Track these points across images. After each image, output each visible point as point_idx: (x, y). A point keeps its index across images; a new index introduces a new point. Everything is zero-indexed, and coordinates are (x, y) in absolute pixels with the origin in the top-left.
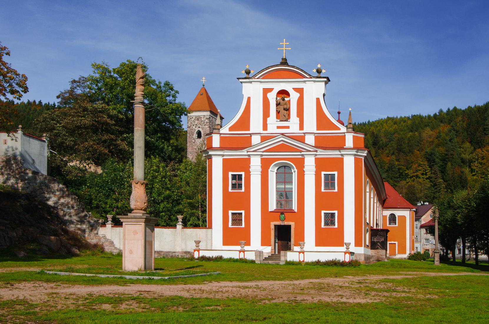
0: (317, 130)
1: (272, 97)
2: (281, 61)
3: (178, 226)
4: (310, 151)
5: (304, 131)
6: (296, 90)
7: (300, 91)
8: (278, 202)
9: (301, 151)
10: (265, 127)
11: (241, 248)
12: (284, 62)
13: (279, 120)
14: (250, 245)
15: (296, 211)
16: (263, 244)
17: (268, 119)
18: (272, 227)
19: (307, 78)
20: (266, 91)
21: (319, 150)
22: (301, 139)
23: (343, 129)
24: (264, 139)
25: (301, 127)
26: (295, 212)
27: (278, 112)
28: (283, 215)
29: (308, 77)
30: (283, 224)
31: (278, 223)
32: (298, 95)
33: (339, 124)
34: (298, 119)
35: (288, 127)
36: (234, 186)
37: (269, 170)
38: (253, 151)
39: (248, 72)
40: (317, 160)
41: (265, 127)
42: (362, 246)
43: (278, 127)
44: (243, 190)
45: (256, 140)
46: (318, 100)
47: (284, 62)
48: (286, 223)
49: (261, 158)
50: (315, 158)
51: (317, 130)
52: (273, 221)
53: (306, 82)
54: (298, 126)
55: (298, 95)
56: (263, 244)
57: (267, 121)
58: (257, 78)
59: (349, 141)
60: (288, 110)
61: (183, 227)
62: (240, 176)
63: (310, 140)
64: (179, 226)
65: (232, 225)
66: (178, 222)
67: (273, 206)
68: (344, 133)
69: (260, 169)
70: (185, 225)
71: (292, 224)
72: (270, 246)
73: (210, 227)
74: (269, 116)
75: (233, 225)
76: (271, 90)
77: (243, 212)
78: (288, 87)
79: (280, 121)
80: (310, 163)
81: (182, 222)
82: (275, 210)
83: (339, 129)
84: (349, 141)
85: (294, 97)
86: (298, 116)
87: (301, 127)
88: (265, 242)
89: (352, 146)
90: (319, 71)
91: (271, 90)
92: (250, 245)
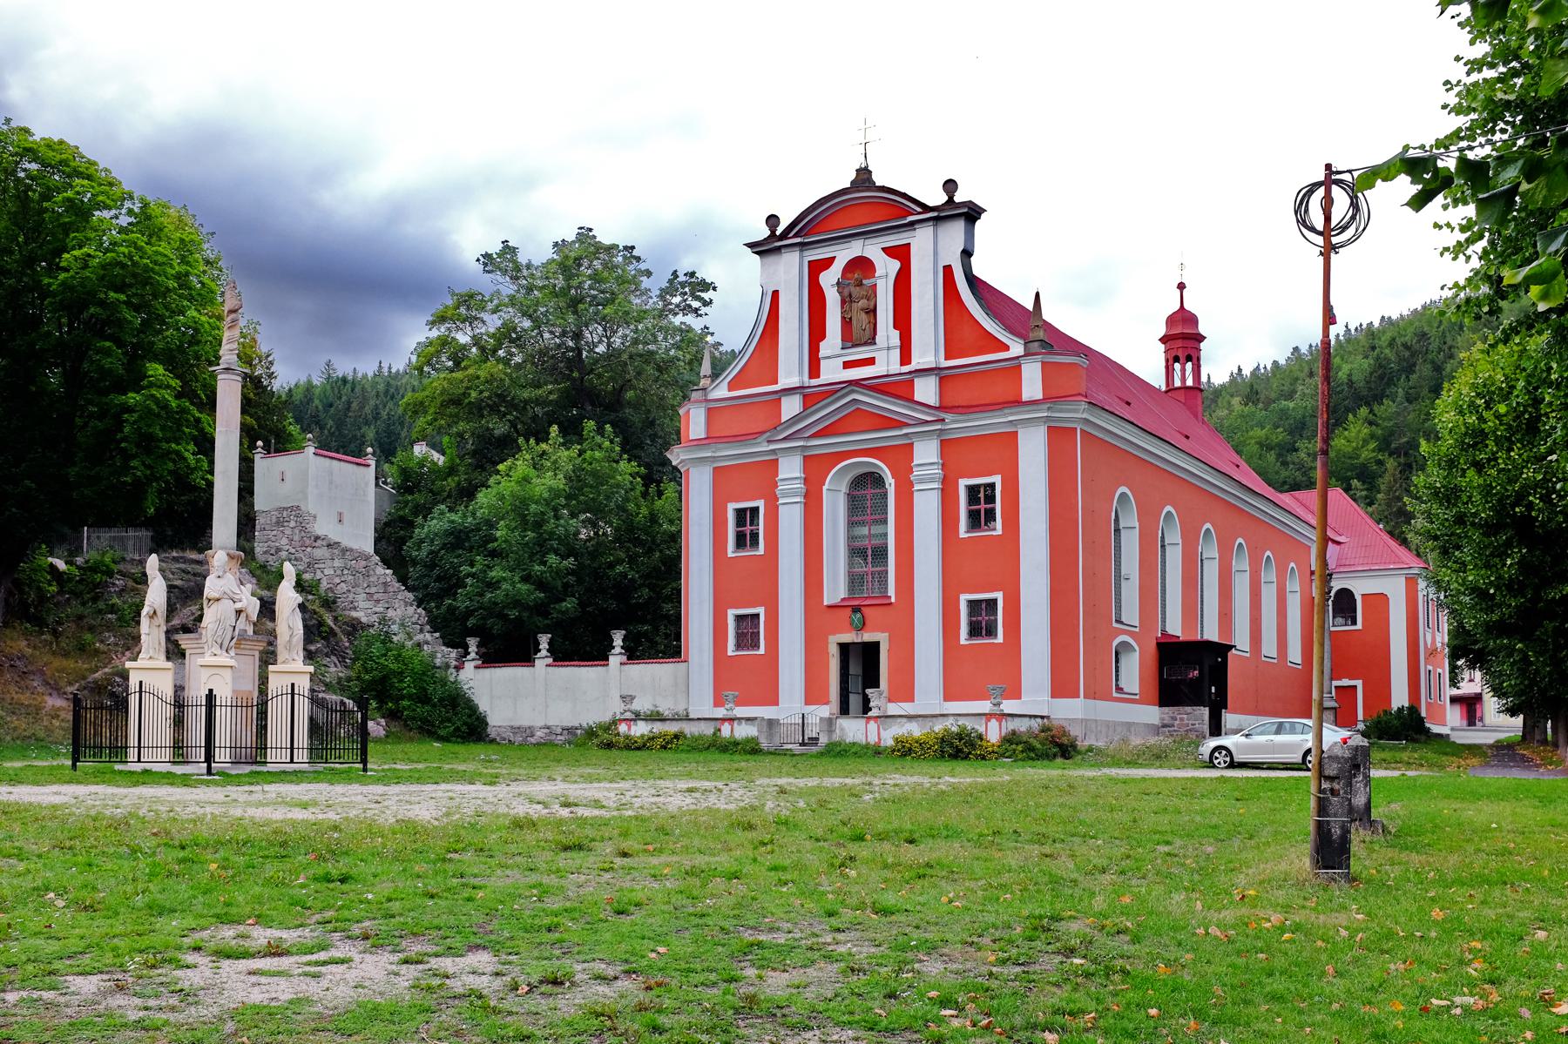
0: (947, 358)
1: (829, 280)
2: (853, 175)
3: (611, 658)
4: (927, 422)
5: (913, 366)
6: (889, 251)
7: (901, 253)
8: (855, 581)
9: (908, 425)
11: (725, 712)
12: (864, 176)
13: (850, 344)
14: (912, 700)
15: (893, 600)
16: (809, 700)
17: (822, 344)
18: (834, 651)
19: (919, 213)
21: (948, 417)
22: (898, 388)
23: (1017, 348)
24: (811, 398)
25: (906, 357)
26: (891, 604)
27: (846, 323)
28: (859, 615)
29: (919, 210)
30: (859, 641)
31: (848, 637)
32: (895, 265)
33: (997, 328)
34: (898, 332)
35: (871, 361)
36: (741, 541)
37: (825, 488)
38: (785, 439)
39: (772, 220)
40: (945, 445)
41: (814, 371)
42: (1078, 697)
43: (847, 365)
44: (761, 550)
45: (791, 407)
46: (948, 270)
47: (864, 176)
48: (868, 637)
49: (804, 457)
50: (941, 441)
51: (947, 358)
52: (834, 633)
53: (916, 226)
54: (896, 354)
55: (895, 265)
56: (809, 700)
58: (795, 236)
59: (1032, 383)
61: (624, 658)
62: (755, 510)
63: (926, 391)
64: (616, 658)
65: (737, 650)
66: (614, 648)
67: (835, 589)
68: (1018, 358)
69: (799, 485)
70: (562, 655)
71: (882, 638)
72: (827, 703)
74: (823, 336)
75: (739, 646)
77: (761, 610)
78: (872, 250)
79: (854, 346)
80: (926, 454)
81: (622, 647)
82: (843, 600)
83: (1006, 348)
84: (1032, 383)
85: (887, 268)
87: (906, 357)
88: (813, 695)
89: (1040, 396)
90: (950, 186)
92: (912, 700)
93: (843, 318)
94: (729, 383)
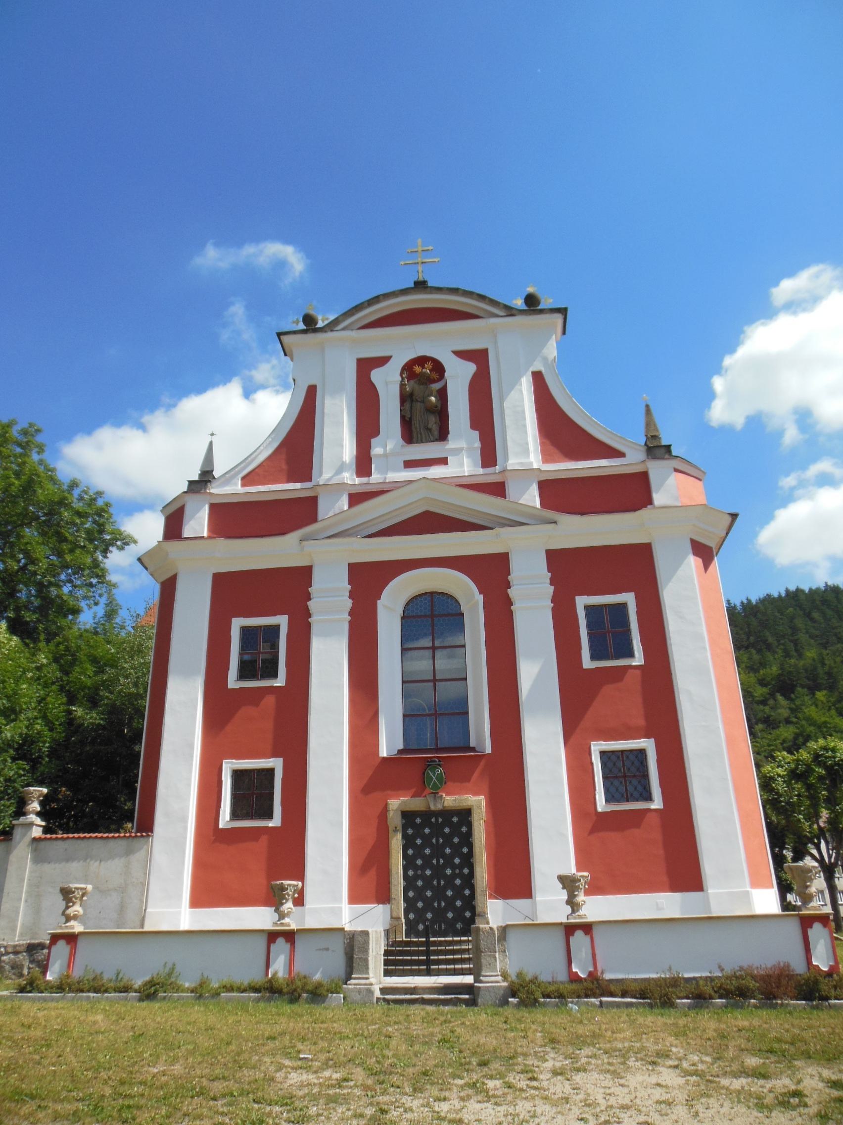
7: (479, 357)
10: (363, 464)
20: (365, 366)
25: (489, 456)
31: (417, 804)
32: (471, 368)
34: (476, 434)
35: (444, 461)
43: (409, 464)
48: (450, 800)
55: (471, 368)
57: (369, 447)
60: (442, 412)
73: (146, 827)
74: (376, 432)
76: (382, 361)
86: (474, 426)
87: (489, 456)
91: (382, 361)
93: (403, 417)
94: (243, 478)
